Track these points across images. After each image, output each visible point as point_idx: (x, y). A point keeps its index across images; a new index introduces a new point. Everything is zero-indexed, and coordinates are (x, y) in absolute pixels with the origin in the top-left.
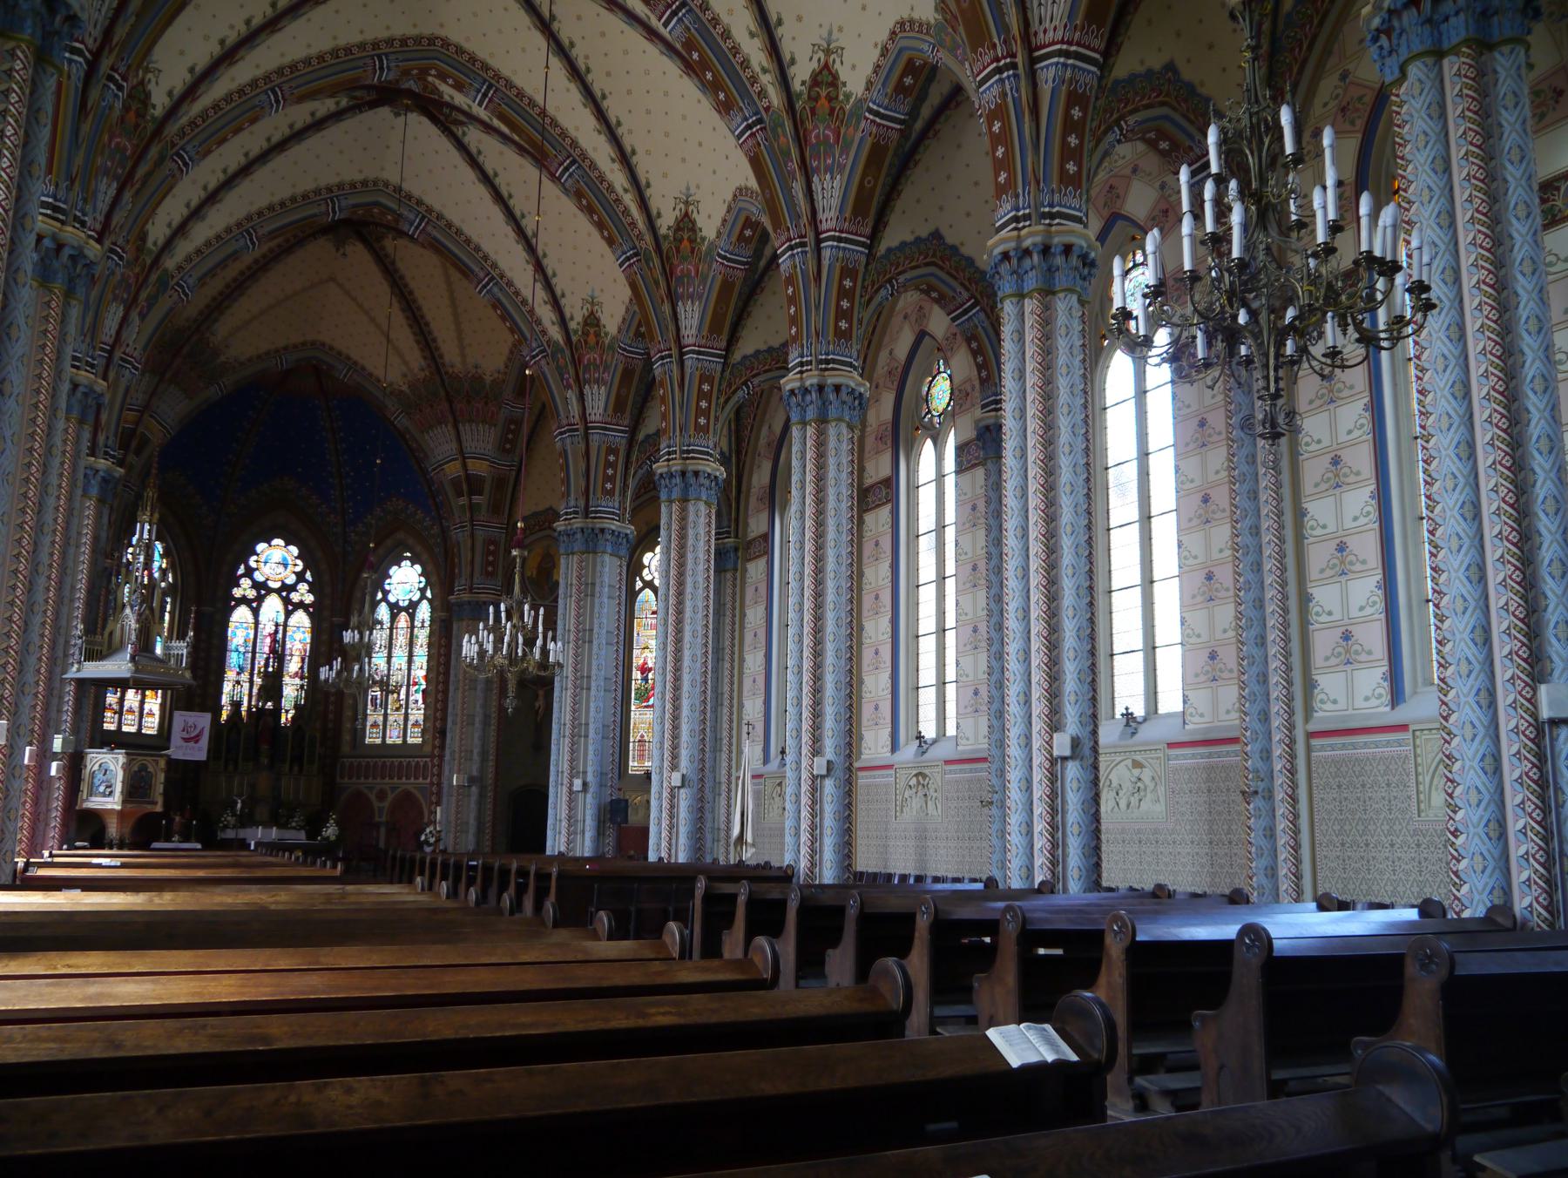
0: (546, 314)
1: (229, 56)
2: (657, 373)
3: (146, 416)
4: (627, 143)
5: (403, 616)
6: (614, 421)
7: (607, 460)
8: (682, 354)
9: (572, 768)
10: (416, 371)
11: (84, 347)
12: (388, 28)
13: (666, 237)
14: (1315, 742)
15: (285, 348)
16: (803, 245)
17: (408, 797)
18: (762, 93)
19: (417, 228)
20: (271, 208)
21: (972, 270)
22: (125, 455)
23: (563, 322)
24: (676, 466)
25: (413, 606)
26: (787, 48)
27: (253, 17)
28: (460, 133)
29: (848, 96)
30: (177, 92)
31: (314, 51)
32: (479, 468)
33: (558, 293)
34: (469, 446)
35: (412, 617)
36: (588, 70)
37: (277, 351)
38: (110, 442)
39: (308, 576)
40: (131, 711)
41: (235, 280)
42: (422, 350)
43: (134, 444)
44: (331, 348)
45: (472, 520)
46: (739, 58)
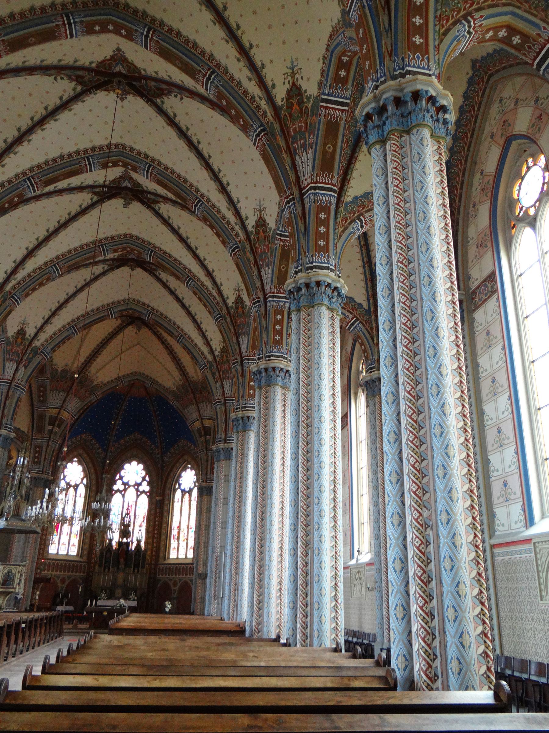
0: (205, 349)
1: (30, 254)
3: (62, 411)
4: (210, 267)
5: (187, 495)
9: (216, 569)
13: (232, 307)
14: (496, 551)
16: (258, 302)
17: (186, 583)
18: (237, 235)
21: (353, 304)
23: (212, 352)
24: (240, 414)
25: (191, 490)
28: (158, 274)
29: (270, 229)
30: (9, 272)
31: (72, 247)
32: (208, 423)
33: (209, 339)
35: (190, 495)
36: (188, 238)
38: (9, 422)
39: (147, 478)
41: (95, 349)
43: (57, 423)
44: (144, 374)
45: (206, 448)
46: (226, 221)
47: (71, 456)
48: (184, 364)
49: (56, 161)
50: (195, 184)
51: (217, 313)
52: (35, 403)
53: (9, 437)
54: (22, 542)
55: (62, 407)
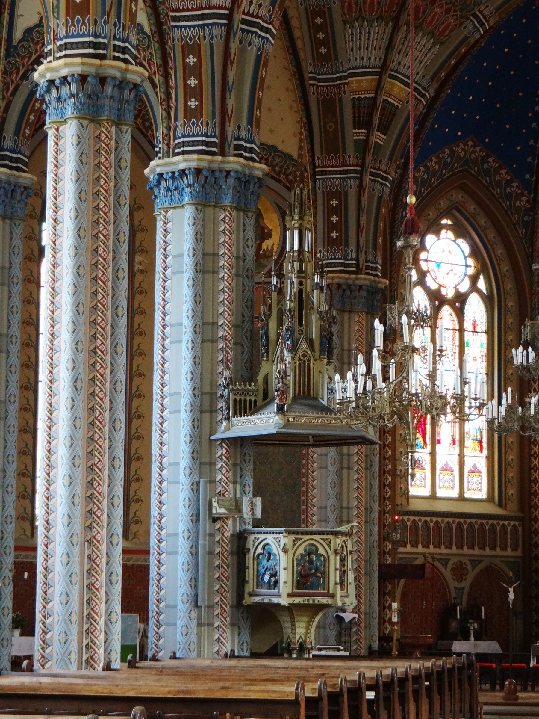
11: (109, 29)
22: (368, 135)
38: (243, 133)
40: (447, 469)
43: (376, 119)
47: (432, 214)
52: (308, 66)
53: (251, 176)
54: (332, 469)
55: (384, 66)
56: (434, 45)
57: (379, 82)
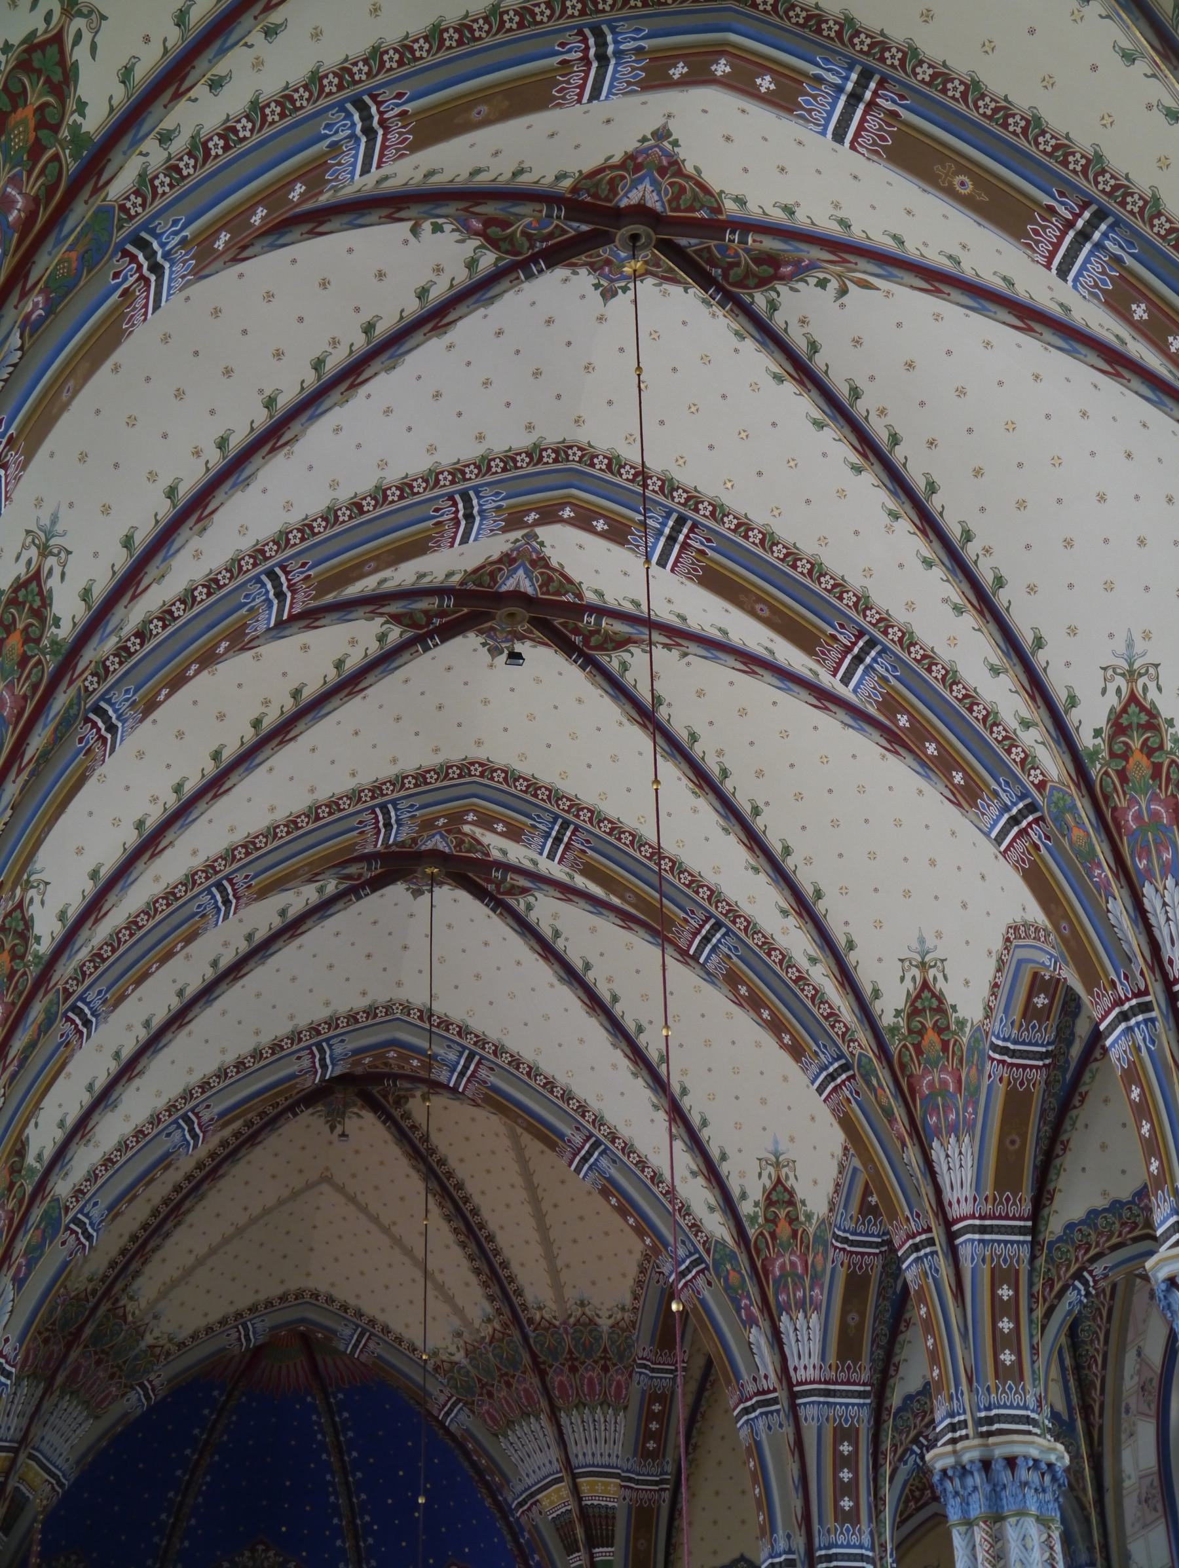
2: (909, 1276)
3: (22, 1456)
4: (805, 881)
6: (842, 1376)
7: (836, 1453)
8: (951, 1236)
10: (477, 1323)
12: (394, 761)
13: (894, 1030)
15: (253, 1309)
16: (1146, 1008)
18: (1028, 762)
19: (462, 1074)
20: (222, 1074)
23: (728, 1204)
26: (1058, 683)
27: (185, 779)
28: (521, 908)
30: (72, 914)
31: (280, 815)
33: (715, 1153)
34: (581, 1452)
37: (239, 1315)
41: (166, 1201)
42: (485, 1285)
44: (330, 1299)
48: (507, 1253)
49: (359, 506)
50: (855, 581)
51: (833, 1051)
55: (24, 1440)
56: (87, 1418)
57: (13, 1462)
